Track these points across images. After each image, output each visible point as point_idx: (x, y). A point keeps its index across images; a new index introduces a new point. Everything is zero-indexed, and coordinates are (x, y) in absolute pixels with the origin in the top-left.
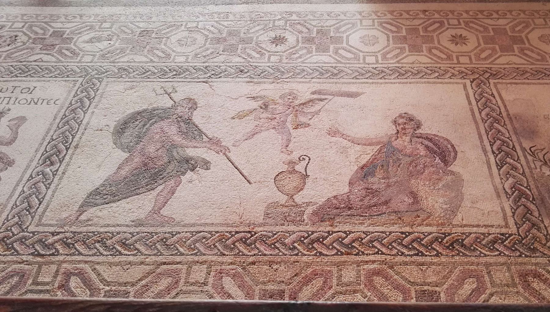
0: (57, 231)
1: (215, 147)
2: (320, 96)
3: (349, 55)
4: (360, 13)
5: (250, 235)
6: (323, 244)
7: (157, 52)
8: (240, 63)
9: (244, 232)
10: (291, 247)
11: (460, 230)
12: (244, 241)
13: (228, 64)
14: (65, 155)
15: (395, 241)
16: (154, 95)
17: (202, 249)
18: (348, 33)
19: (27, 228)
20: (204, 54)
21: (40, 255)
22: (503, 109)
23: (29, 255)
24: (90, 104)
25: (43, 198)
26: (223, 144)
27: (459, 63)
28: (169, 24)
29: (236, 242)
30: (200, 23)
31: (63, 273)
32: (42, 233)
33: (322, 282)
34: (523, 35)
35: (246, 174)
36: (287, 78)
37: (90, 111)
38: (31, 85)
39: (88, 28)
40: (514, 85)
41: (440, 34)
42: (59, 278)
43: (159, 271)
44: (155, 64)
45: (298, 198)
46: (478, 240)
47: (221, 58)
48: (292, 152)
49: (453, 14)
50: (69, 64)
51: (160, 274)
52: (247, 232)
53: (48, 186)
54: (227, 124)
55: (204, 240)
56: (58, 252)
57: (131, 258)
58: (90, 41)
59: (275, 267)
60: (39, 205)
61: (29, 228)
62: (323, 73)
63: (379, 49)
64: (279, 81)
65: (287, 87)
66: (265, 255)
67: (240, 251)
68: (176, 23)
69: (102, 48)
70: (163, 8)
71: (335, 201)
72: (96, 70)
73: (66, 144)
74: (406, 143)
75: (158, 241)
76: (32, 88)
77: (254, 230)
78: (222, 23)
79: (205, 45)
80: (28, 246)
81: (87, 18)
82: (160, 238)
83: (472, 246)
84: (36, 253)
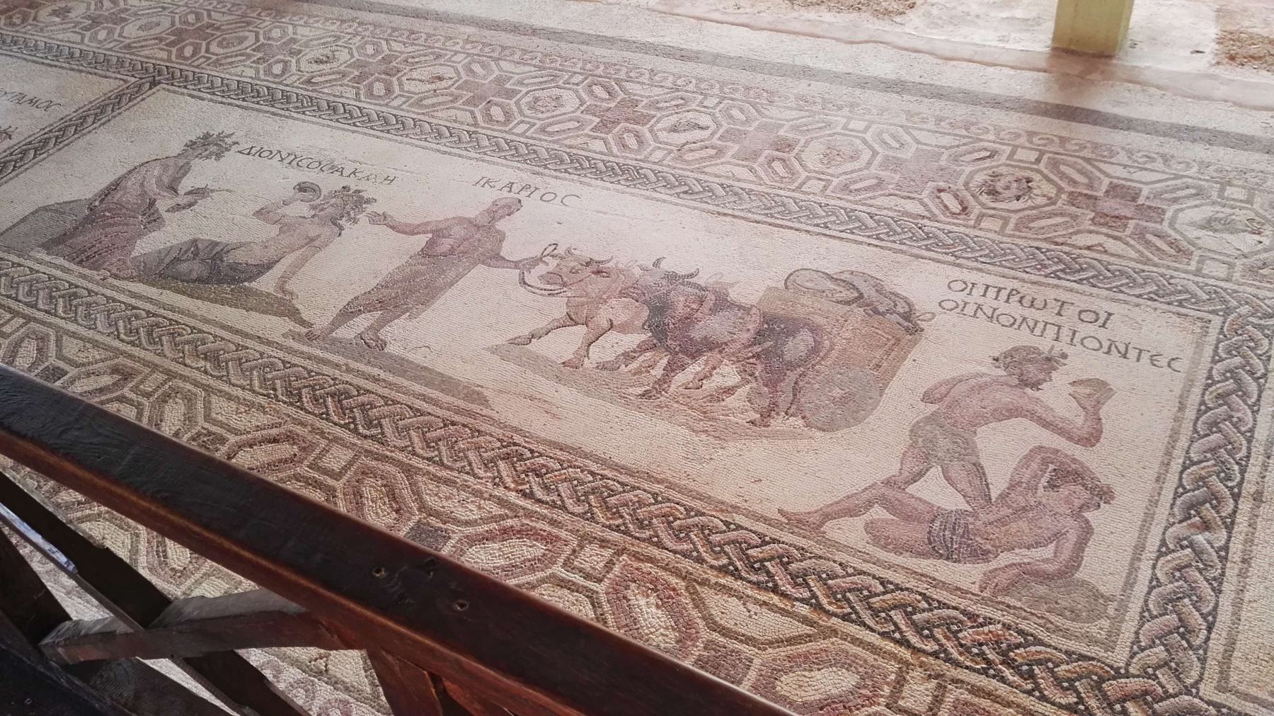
38: (1104, 306)
39: (1193, 191)
50: (1175, 274)
58: (1208, 225)
61: (1202, 686)
72: (1247, 303)
73: (1230, 484)
76: (1103, 317)
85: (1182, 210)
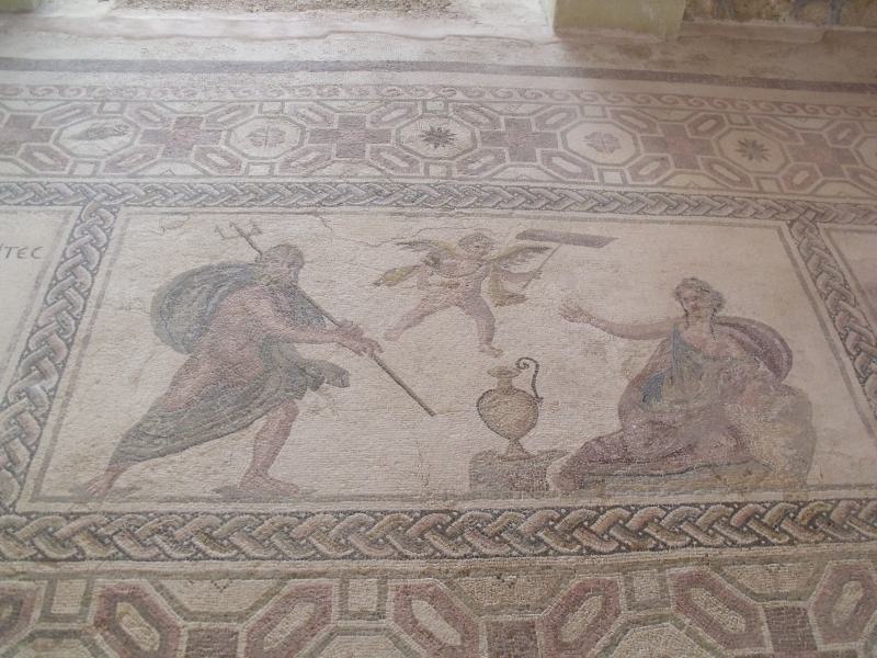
0: (74, 510)
1: (351, 342)
2: (534, 244)
3: (573, 168)
4: (578, 94)
5: (449, 518)
6: (592, 532)
7: (214, 157)
8: (375, 177)
9: (437, 512)
10: (533, 539)
11: (821, 495)
12: (441, 531)
13: (351, 180)
14: (66, 358)
15: (717, 520)
16: (219, 238)
17: (361, 546)
18: (563, 128)
19: (13, 505)
20: (303, 161)
21: (46, 560)
22: (848, 278)
23: (26, 559)
24: (101, 257)
25: (36, 444)
26: (365, 336)
27: (761, 191)
28: (229, 105)
29: (424, 532)
30: (287, 104)
31: (100, 596)
32: (44, 514)
33: (600, 603)
34: (851, 147)
35: (422, 397)
36: (466, 208)
37: (104, 268)
39: (78, 111)
40: (856, 235)
41: (720, 137)
42: (94, 607)
43: (285, 590)
44: (212, 180)
45: (531, 443)
46: (853, 512)
47: (337, 168)
48: (500, 351)
49: (733, 104)
50: (49, 179)
51: (288, 596)
52: (442, 512)
53: (42, 419)
54: (367, 295)
55: (363, 529)
56: (83, 554)
57: (228, 565)
58: (86, 136)
59: (508, 579)
60: (31, 459)
61: (18, 504)
62: (531, 198)
63: (624, 159)
64: (452, 212)
65: (469, 225)
66: (485, 556)
67: (437, 550)
68: (242, 104)
69: (110, 149)
70: (213, 77)
71: (598, 448)
72: (104, 191)
73: (66, 337)
74: (704, 336)
75: (275, 532)
77: (456, 508)
78: (328, 103)
79: (301, 143)
80: (22, 543)
81: (71, 93)
82: (277, 524)
83: (844, 523)
84: (40, 556)
85: (65, 128)
